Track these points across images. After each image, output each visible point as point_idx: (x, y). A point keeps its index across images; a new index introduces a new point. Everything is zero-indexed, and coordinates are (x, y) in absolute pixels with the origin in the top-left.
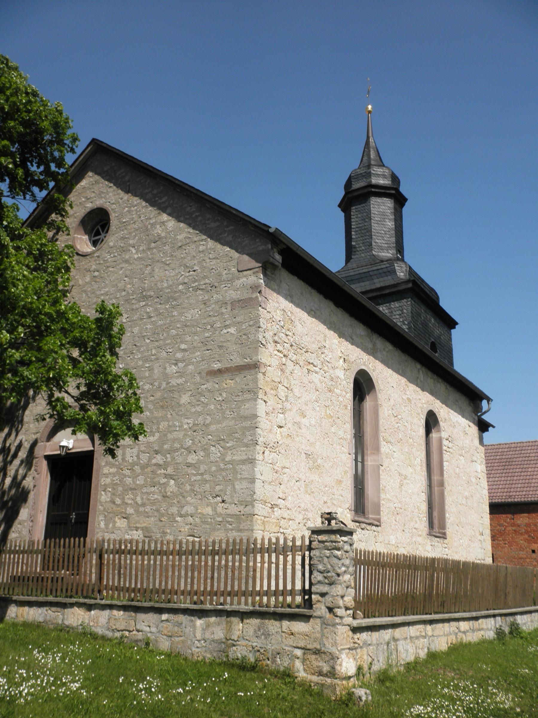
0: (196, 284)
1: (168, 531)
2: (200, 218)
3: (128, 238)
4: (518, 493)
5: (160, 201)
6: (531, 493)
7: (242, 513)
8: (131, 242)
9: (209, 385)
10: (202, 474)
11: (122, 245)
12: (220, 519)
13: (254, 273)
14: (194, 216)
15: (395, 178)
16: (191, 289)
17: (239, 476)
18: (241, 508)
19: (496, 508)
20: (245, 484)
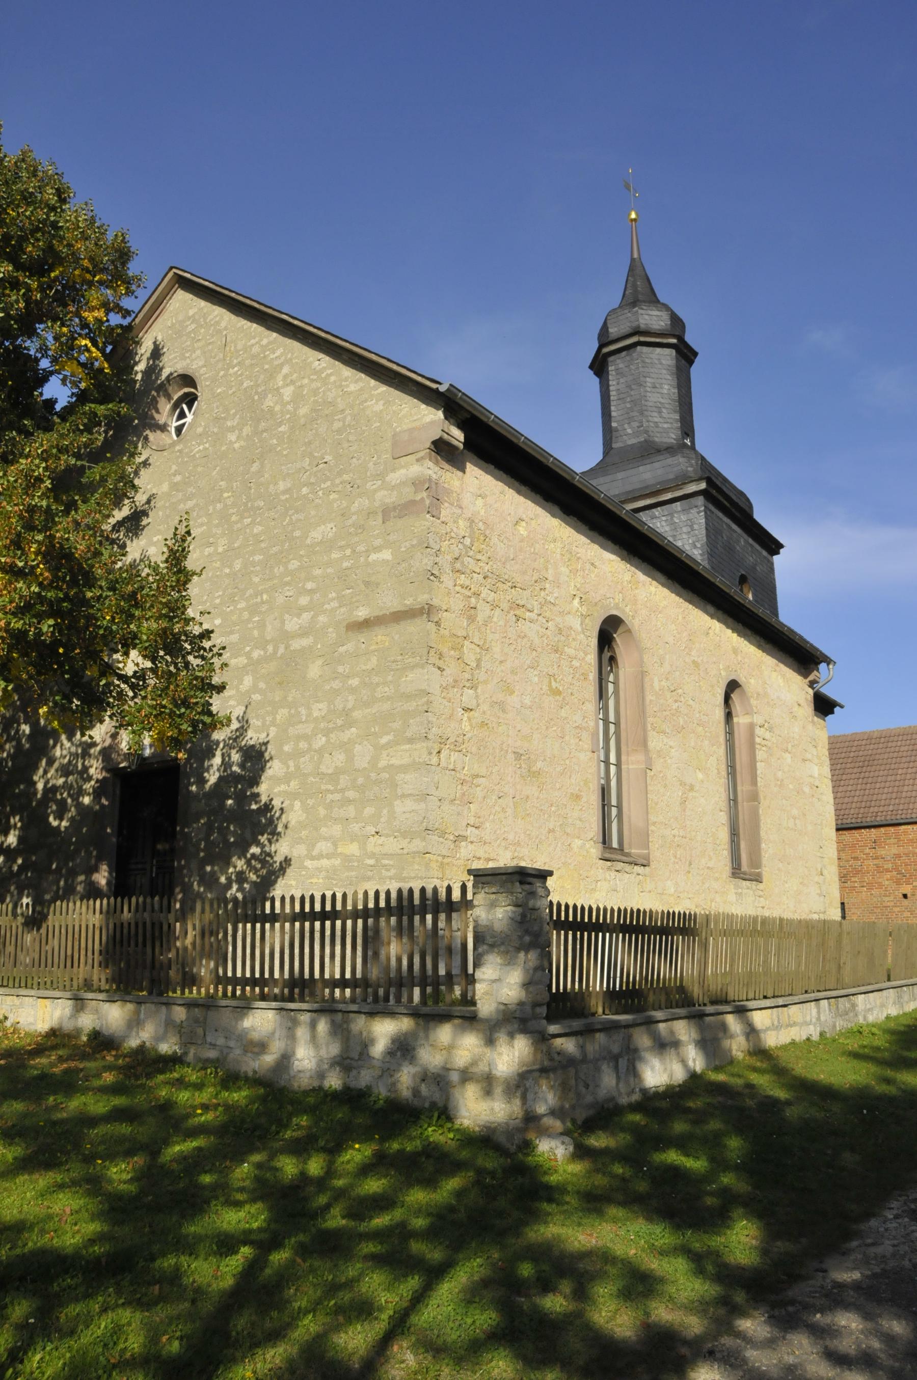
0: (329, 483)
1: (293, 883)
2: (333, 379)
3: (224, 418)
4: (881, 809)
5: (272, 356)
6: (901, 807)
7: (405, 851)
8: (229, 424)
9: (349, 647)
10: (342, 791)
11: (216, 430)
12: (371, 862)
13: (418, 460)
14: (323, 375)
15: (677, 322)
16: (320, 493)
17: (399, 792)
18: (404, 843)
19: (838, 830)
20: (410, 804)
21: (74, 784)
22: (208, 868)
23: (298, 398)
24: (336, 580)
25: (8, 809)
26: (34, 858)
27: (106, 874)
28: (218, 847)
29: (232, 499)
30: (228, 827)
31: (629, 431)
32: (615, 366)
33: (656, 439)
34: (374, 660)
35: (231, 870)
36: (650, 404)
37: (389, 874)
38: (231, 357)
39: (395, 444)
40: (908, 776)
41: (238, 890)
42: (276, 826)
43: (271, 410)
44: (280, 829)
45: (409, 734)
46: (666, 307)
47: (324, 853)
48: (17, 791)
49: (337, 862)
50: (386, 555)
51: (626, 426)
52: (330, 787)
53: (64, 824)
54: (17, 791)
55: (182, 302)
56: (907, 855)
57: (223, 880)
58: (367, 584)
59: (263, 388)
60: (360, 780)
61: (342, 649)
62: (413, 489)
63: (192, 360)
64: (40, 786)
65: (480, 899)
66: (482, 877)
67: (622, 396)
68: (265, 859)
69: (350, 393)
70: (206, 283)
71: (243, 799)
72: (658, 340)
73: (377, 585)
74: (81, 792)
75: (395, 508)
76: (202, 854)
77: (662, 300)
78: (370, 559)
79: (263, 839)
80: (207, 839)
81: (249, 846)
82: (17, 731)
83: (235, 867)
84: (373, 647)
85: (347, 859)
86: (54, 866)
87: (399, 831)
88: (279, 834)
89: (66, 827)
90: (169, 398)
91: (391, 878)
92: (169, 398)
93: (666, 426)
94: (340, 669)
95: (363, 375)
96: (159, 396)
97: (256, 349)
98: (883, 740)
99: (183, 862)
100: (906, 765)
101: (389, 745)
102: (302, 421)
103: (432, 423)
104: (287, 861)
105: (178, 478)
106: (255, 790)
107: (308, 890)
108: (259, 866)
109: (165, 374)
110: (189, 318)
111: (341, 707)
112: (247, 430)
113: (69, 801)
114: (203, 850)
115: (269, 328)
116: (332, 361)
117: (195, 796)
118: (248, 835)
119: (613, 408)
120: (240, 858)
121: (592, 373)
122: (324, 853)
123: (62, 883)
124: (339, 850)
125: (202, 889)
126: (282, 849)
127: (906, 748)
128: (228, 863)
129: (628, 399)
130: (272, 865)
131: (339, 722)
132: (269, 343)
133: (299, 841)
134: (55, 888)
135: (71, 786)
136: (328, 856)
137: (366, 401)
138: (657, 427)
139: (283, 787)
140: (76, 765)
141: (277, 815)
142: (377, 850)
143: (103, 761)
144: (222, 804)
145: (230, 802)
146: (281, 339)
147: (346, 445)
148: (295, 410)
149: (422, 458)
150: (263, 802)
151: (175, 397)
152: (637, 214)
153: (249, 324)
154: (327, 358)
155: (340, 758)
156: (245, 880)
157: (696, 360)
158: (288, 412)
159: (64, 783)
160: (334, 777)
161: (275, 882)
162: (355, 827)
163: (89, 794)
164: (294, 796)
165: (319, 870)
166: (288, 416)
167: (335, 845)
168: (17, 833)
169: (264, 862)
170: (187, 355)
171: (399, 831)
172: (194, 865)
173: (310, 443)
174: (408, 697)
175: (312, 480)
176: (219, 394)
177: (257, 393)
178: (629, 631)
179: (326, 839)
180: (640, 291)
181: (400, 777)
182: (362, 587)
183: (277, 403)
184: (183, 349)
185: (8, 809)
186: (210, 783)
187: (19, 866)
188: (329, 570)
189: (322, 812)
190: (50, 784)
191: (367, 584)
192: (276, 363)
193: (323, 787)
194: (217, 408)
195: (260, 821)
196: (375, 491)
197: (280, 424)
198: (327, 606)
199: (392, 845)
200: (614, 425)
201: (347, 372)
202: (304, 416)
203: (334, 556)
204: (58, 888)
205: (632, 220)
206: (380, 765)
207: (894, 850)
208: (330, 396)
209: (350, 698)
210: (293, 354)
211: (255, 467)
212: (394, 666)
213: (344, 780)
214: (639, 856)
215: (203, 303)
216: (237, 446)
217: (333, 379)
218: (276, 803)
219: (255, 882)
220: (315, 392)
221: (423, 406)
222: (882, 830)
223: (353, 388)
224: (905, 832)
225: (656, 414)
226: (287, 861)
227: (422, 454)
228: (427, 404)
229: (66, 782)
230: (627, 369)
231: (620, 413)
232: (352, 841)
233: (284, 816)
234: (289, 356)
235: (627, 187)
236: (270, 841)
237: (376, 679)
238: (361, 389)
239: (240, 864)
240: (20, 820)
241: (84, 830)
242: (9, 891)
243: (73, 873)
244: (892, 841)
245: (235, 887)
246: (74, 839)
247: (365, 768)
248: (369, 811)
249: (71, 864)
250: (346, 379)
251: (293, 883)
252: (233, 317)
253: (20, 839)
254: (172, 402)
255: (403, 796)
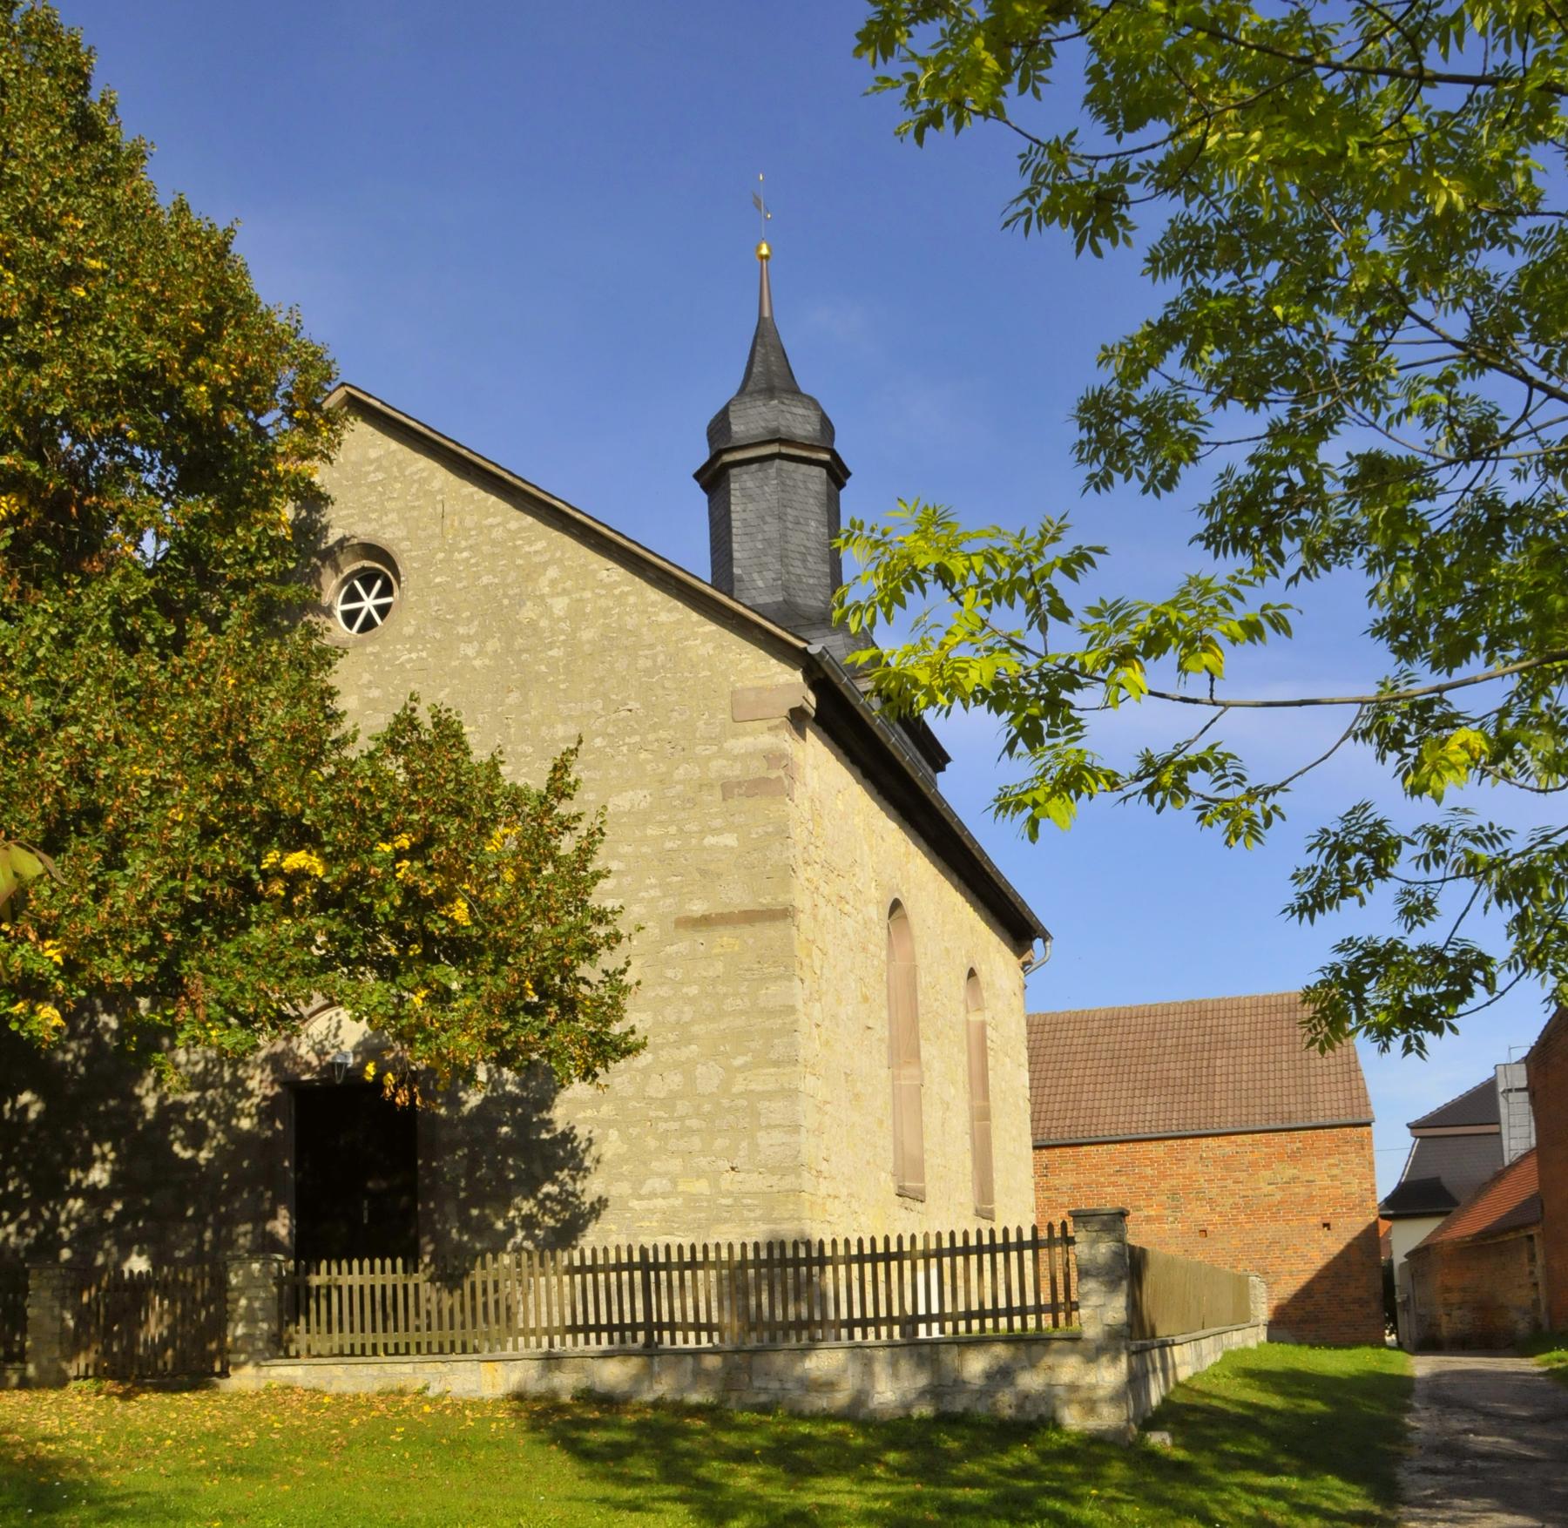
0: (637, 738)
1: (614, 1227)
2: (632, 599)
3: (451, 621)
4: (1055, 1123)
5: (527, 549)
6: (1081, 1121)
7: (775, 1189)
8: (461, 630)
9: (682, 947)
10: (682, 1119)
11: (438, 636)
12: (729, 1201)
13: (770, 729)
14: (617, 592)
15: (827, 426)
16: (625, 749)
17: (763, 1122)
18: (774, 1180)
20: (778, 1136)
21: (218, 1100)
22: (475, 1212)
23: (577, 614)
24: (656, 863)
25: (86, 1133)
26: (147, 1202)
27: (287, 1222)
28: (489, 1184)
29: (478, 736)
30: (504, 1160)
31: (760, 583)
32: (741, 484)
33: (799, 600)
34: (720, 967)
35: (512, 1213)
36: (792, 547)
37: (752, 1215)
38: (455, 536)
39: (734, 705)
40: (1087, 1080)
41: (525, 1238)
42: (582, 1160)
43: (533, 624)
44: (587, 1163)
45: (773, 1056)
46: (813, 403)
47: (659, 1191)
48: (102, 1108)
49: (678, 1202)
50: (730, 840)
51: (755, 576)
52: (662, 1114)
53: (204, 1155)
54: (102, 1108)
55: (360, 438)
56: (1089, 1185)
57: (500, 1225)
58: (704, 873)
59: (517, 591)
60: (707, 1107)
61: (669, 949)
62: (765, 765)
63: (383, 527)
64: (150, 1102)
65: (1080, 1236)
66: (1080, 1217)
67: (749, 530)
68: (566, 1199)
69: (661, 625)
70: (413, 424)
71: (523, 1126)
72: (805, 454)
73: (719, 875)
74: (232, 1111)
75: (739, 784)
76: (462, 1195)
77: (804, 390)
78: (706, 842)
79: (563, 1175)
80: (469, 1174)
81: (542, 1184)
82: (92, 1023)
83: (519, 1210)
84: (716, 951)
85: (692, 1200)
86: (190, 1212)
87: (765, 1166)
88: (587, 1169)
89: (208, 1160)
90: (337, 569)
91: (756, 1220)
92: (337, 569)
93: (811, 581)
94: (670, 973)
95: (680, 604)
96: (323, 566)
97: (497, 534)
98: (1047, 1028)
99: (432, 1205)
100: (1082, 1064)
101: (745, 1067)
102: (587, 648)
103: (789, 685)
104: (601, 1204)
105: (375, 693)
106: (545, 1115)
107: (636, 1235)
108: (558, 1208)
109: (334, 536)
110: (371, 462)
111: (673, 1019)
112: (493, 645)
113: (211, 1124)
114: (464, 1190)
115: (518, 507)
116: (630, 575)
117: (446, 1122)
118: (537, 1168)
119: (735, 546)
120: (526, 1198)
121: (697, 485)
122: (659, 1191)
123: (208, 1235)
124: (680, 1188)
125: (466, 1238)
126: (591, 1188)
127: (1081, 1041)
128: (507, 1205)
129: (760, 537)
130: (578, 1207)
131: (672, 1037)
132: (521, 529)
133: (621, 1177)
134: (194, 1242)
135: (214, 1104)
136: (665, 1196)
137: (687, 639)
138: (800, 582)
139: (589, 1113)
140: (220, 1075)
141: (583, 1146)
142: (735, 1188)
143: (273, 1071)
144: (494, 1134)
145: (505, 1129)
146: (540, 526)
147: (660, 692)
148: (574, 631)
149: (777, 727)
150: (559, 1130)
151: (347, 571)
152: (769, 248)
153: (483, 494)
154: (622, 570)
155: (675, 1080)
156: (538, 1225)
157: (848, 482)
158: (563, 632)
159: (198, 1099)
160: (669, 1102)
161: (585, 1226)
162: (703, 1162)
163: (249, 1115)
164: (608, 1124)
165: (652, 1211)
166: (562, 637)
167: (675, 1183)
168: (108, 1166)
169: (565, 1204)
170: (374, 516)
171: (765, 1166)
172: (450, 1208)
173: (602, 680)
174: (771, 1013)
175: (610, 730)
176: (439, 585)
177: (505, 595)
178: (905, 917)
179: (659, 1175)
180: (770, 373)
181: (763, 1105)
182: (698, 877)
183: (541, 616)
184: (365, 505)
185: (86, 1133)
186: (468, 1106)
187: (117, 1213)
188: (644, 849)
189: (652, 1143)
190: (170, 1100)
191: (704, 873)
192: (536, 559)
193: (652, 1114)
194: (437, 603)
195: (556, 1154)
196: (709, 758)
197: (551, 646)
198: (642, 894)
199: (755, 1182)
200: (737, 571)
201: (654, 595)
202: (589, 642)
203: (649, 832)
204: (202, 1242)
205: (762, 257)
206: (734, 1090)
207: (1072, 1179)
208: (630, 622)
209: (686, 1009)
210: (563, 553)
211: (513, 698)
212: (748, 975)
213: (682, 1107)
214: (914, 1190)
215: (394, 445)
216: (477, 663)
217: (632, 599)
218: (581, 1132)
219: (553, 1228)
220: (606, 612)
221: (773, 661)
222: (1057, 1151)
223: (663, 617)
224: (1087, 1155)
225: (798, 563)
226: (601, 1204)
227: (777, 722)
228: (779, 660)
229: (202, 1097)
230: (758, 491)
231: (746, 555)
232: (699, 1177)
233: (593, 1149)
234: (558, 554)
235: (757, 205)
236: (574, 1179)
237: (722, 989)
238: (679, 622)
239: (528, 1206)
240: (113, 1149)
241: (245, 1164)
242: (101, 1248)
243: (229, 1221)
244: (1070, 1166)
245: (520, 1234)
246: (226, 1176)
247: (712, 1094)
248: (720, 1143)
249: (223, 1209)
250: (653, 604)
251: (614, 1227)
252: (452, 477)
253: (114, 1176)
254: (341, 577)
255: (769, 1127)
